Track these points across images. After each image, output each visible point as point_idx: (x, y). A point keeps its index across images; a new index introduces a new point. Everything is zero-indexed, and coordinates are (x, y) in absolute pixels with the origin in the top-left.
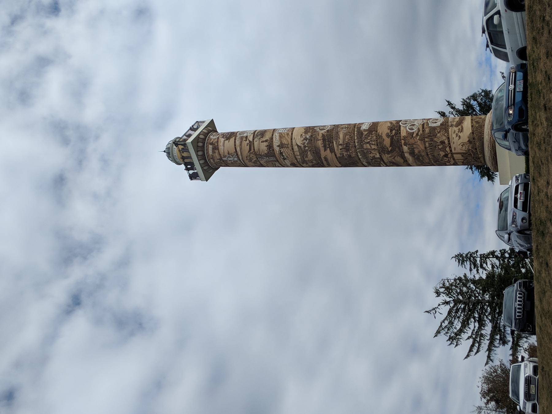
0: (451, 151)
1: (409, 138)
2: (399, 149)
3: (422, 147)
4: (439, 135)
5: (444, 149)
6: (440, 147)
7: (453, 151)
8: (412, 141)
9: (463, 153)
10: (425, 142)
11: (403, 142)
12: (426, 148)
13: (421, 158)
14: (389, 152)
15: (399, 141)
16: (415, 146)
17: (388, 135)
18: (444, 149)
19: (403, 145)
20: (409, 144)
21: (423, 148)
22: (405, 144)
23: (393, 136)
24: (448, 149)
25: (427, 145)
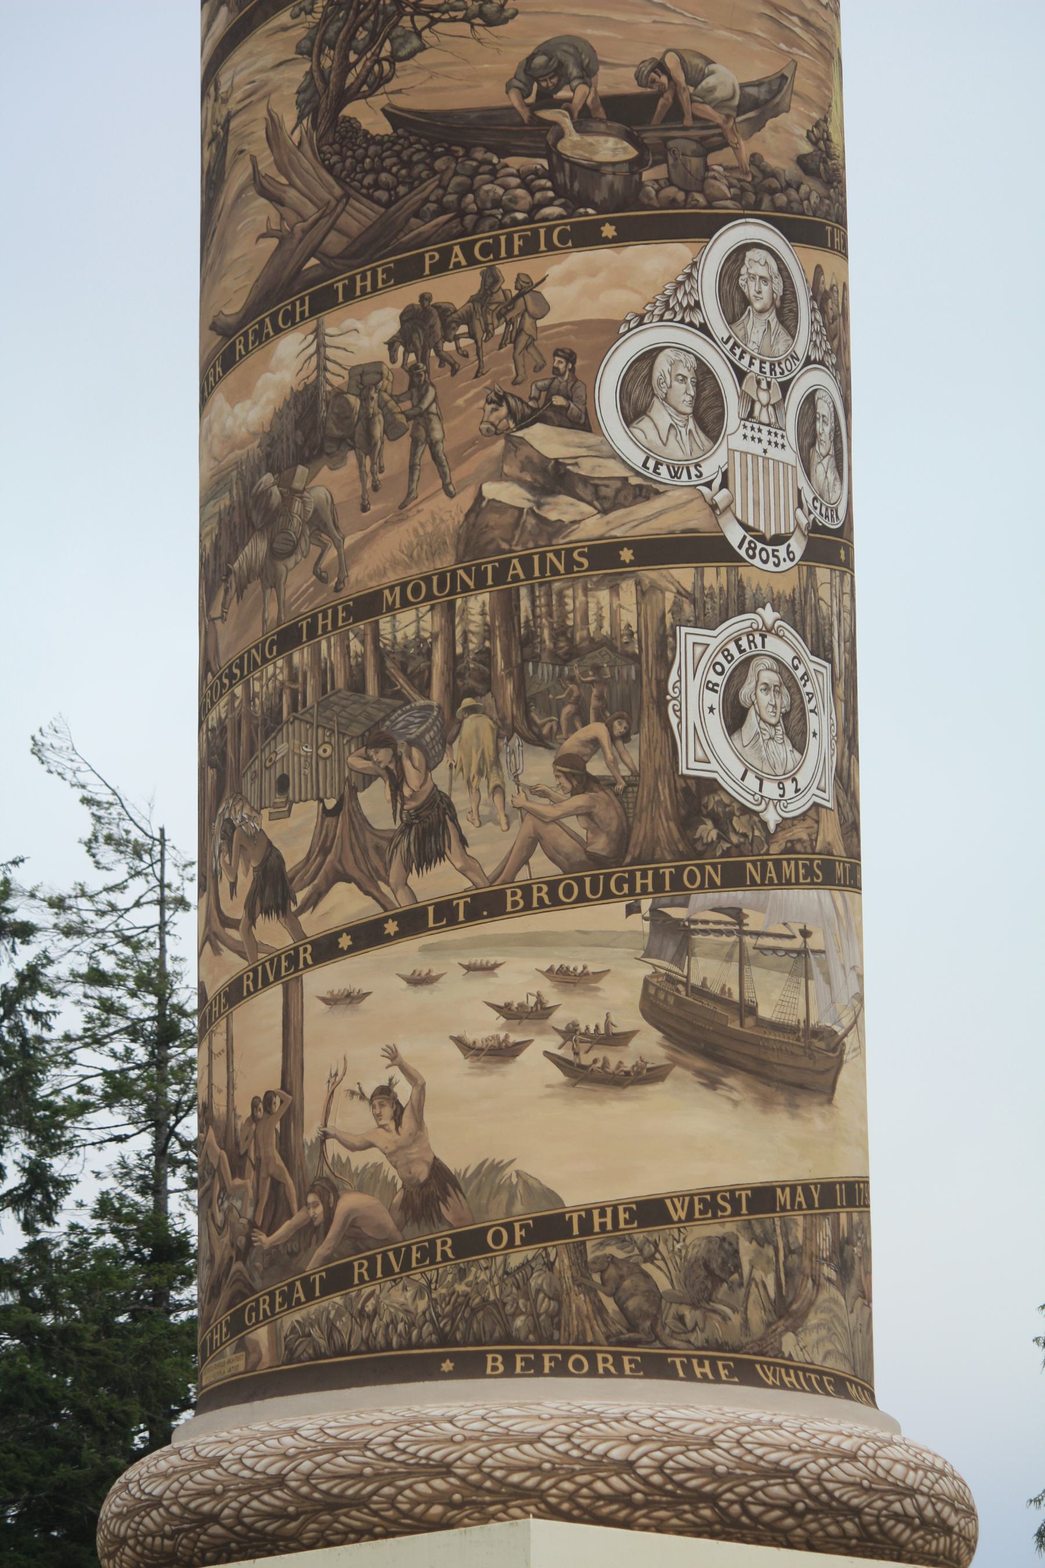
0: (326, 949)
1: (501, 365)
2: (364, 249)
3: (380, 556)
4: (538, 767)
5: (352, 847)
6: (376, 804)
7: (320, 980)
8: (463, 410)
9: (292, 1116)
10: (439, 590)
11: (457, 288)
12: (369, 606)
13: (256, 549)
14: (324, 103)
15: (474, 230)
16: (395, 454)
17: (553, 68)
18: (352, 847)
19: (410, 294)
20: (417, 384)
21: (361, 577)
22: (419, 326)
23: (540, 138)
24: (346, 905)
25: (405, 625)
